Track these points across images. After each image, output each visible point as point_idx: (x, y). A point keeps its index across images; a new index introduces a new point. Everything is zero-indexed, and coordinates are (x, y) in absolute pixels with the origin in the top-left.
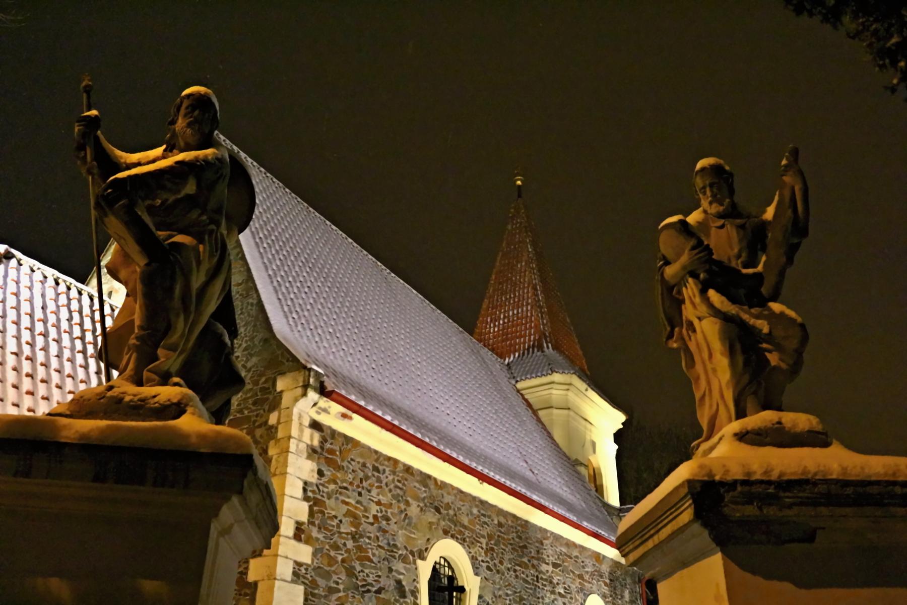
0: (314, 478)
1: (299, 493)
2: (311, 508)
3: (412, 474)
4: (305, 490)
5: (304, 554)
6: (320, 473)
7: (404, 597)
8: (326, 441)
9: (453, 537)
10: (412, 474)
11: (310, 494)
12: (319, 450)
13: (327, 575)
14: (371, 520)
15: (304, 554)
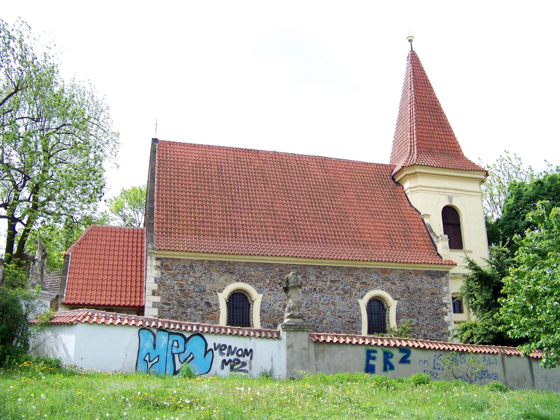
0: (159, 275)
1: (153, 281)
2: (159, 285)
3: (213, 263)
4: (155, 280)
5: (157, 299)
6: (162, 273)
7: (211, 307)
8: (163, 262)
9: (243, 281)
10: (213, 263)
11: (158, 281)
12: (161, 266)
13: (169, 304)
14: (190, 283)
15: (157, 299)
